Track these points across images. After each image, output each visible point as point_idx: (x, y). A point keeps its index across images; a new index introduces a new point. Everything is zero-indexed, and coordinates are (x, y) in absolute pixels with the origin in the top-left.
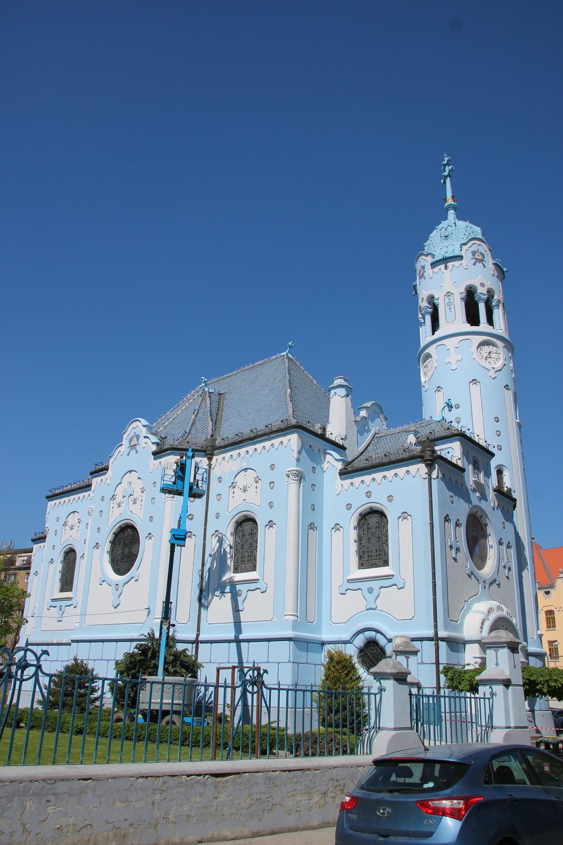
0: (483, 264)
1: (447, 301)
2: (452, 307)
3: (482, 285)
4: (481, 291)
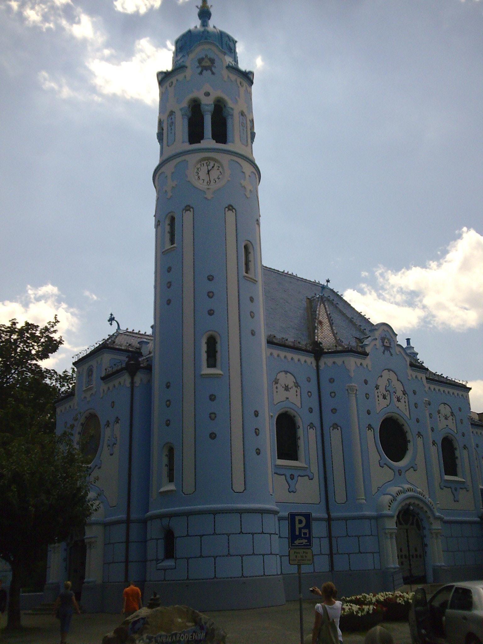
0: (211, 71)
2: (173, 127)
3: (207, 94)
4: (208, 103)
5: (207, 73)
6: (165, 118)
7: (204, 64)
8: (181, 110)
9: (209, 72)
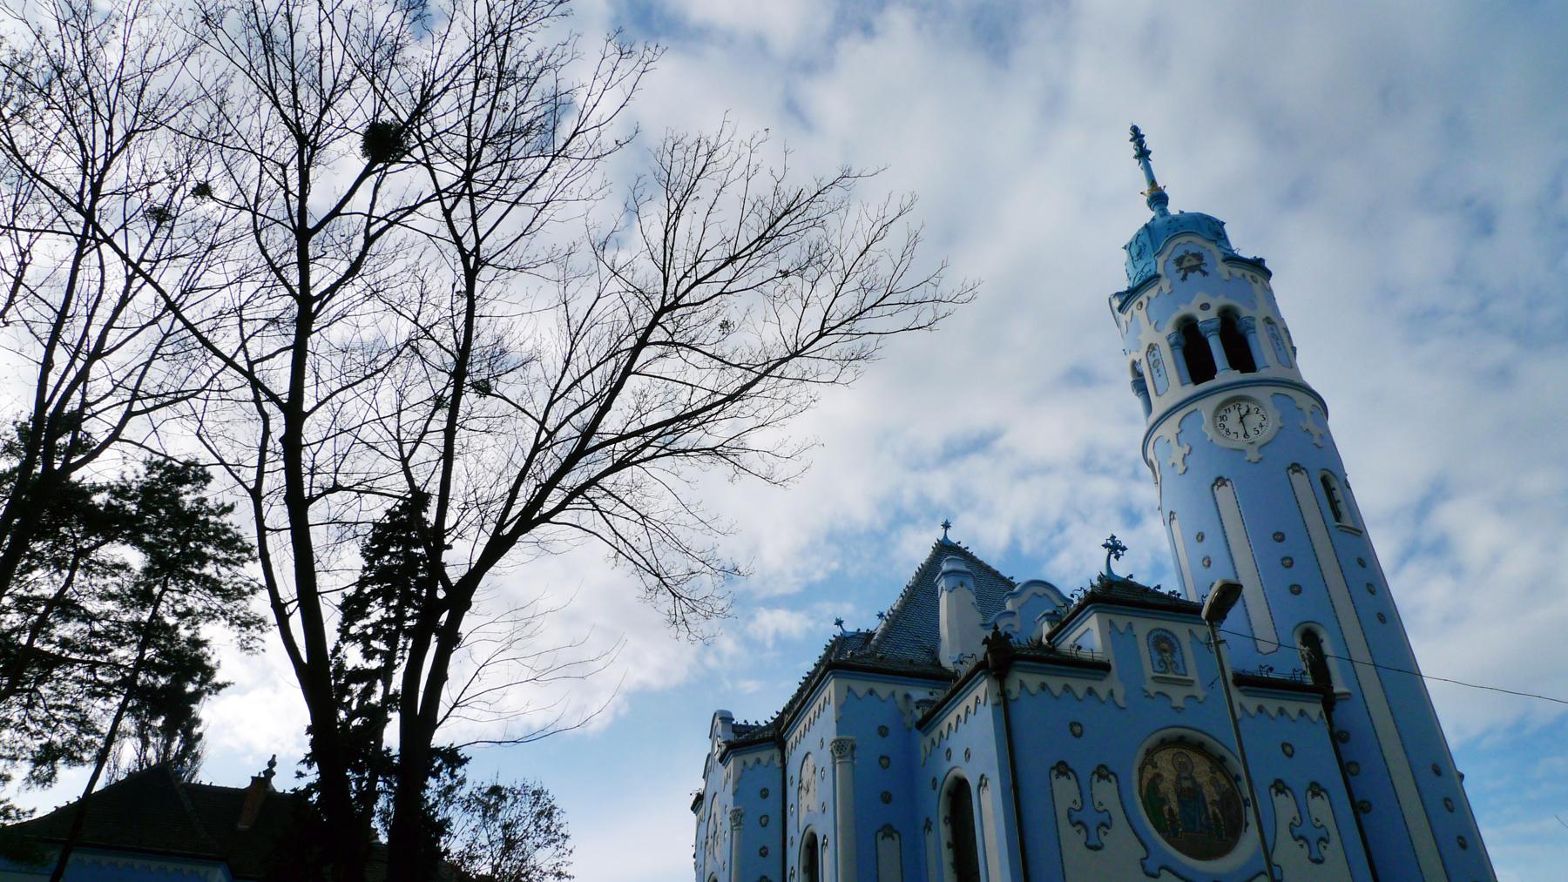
1: (1152, 360)
3: (1205, 307)
5: (1195, 277)
6: (1139, 355)
7: (1186, 264)
8: (1169, 338)
9: (1198, 273)
